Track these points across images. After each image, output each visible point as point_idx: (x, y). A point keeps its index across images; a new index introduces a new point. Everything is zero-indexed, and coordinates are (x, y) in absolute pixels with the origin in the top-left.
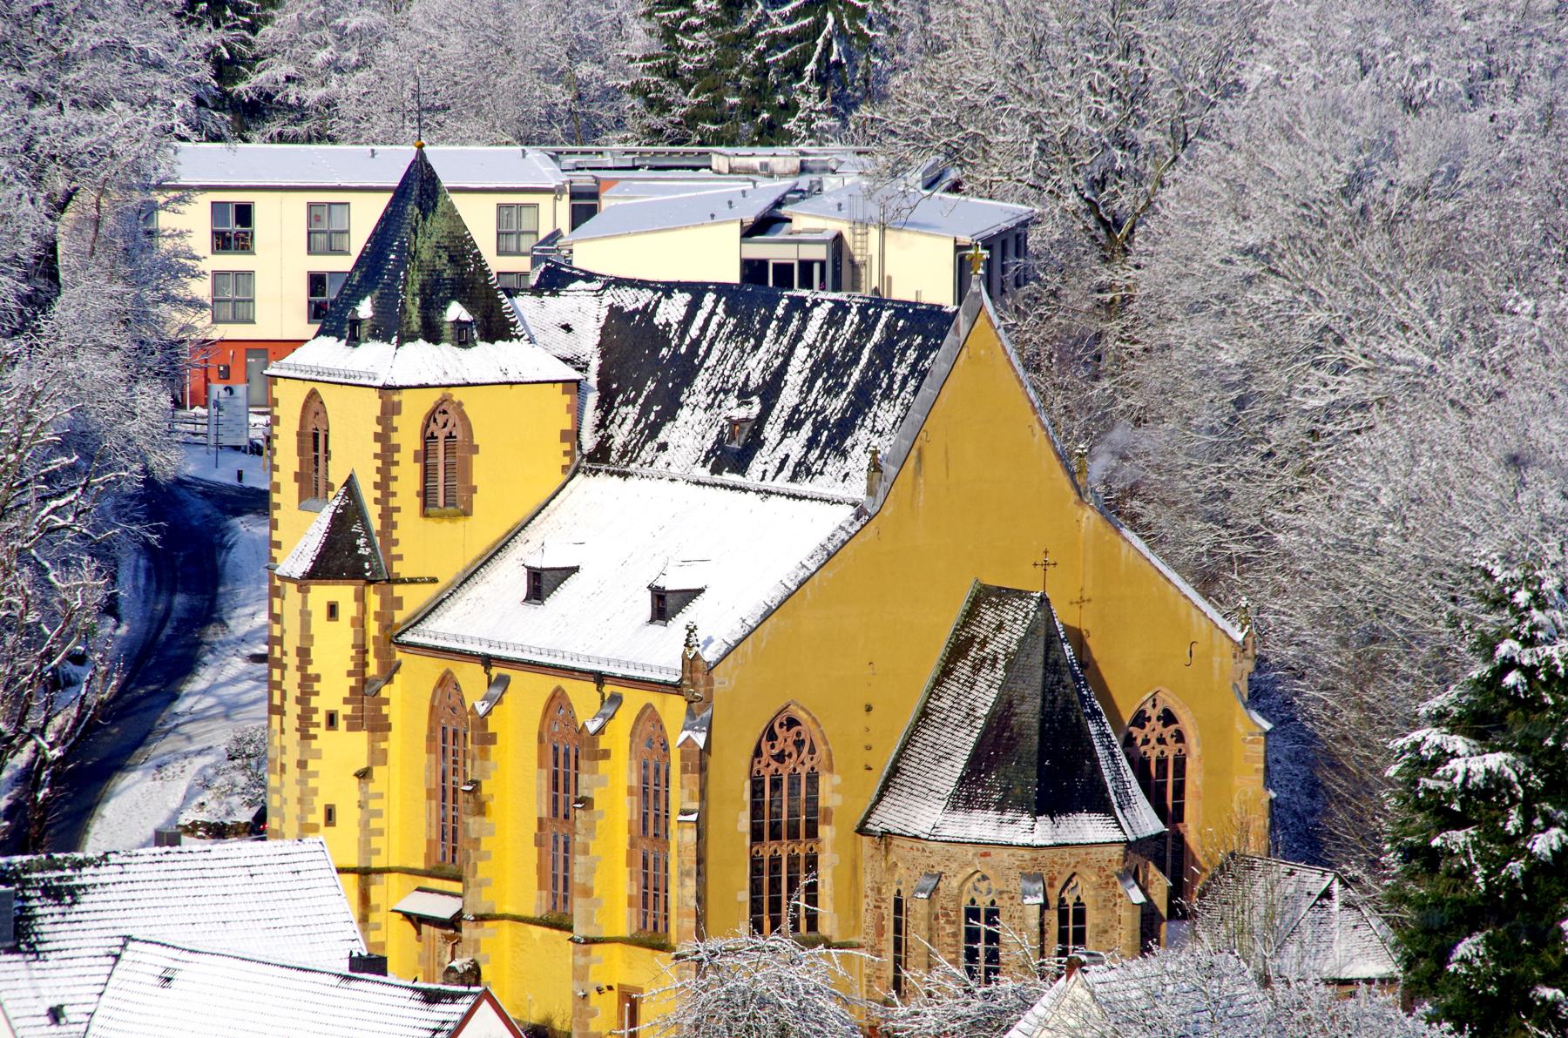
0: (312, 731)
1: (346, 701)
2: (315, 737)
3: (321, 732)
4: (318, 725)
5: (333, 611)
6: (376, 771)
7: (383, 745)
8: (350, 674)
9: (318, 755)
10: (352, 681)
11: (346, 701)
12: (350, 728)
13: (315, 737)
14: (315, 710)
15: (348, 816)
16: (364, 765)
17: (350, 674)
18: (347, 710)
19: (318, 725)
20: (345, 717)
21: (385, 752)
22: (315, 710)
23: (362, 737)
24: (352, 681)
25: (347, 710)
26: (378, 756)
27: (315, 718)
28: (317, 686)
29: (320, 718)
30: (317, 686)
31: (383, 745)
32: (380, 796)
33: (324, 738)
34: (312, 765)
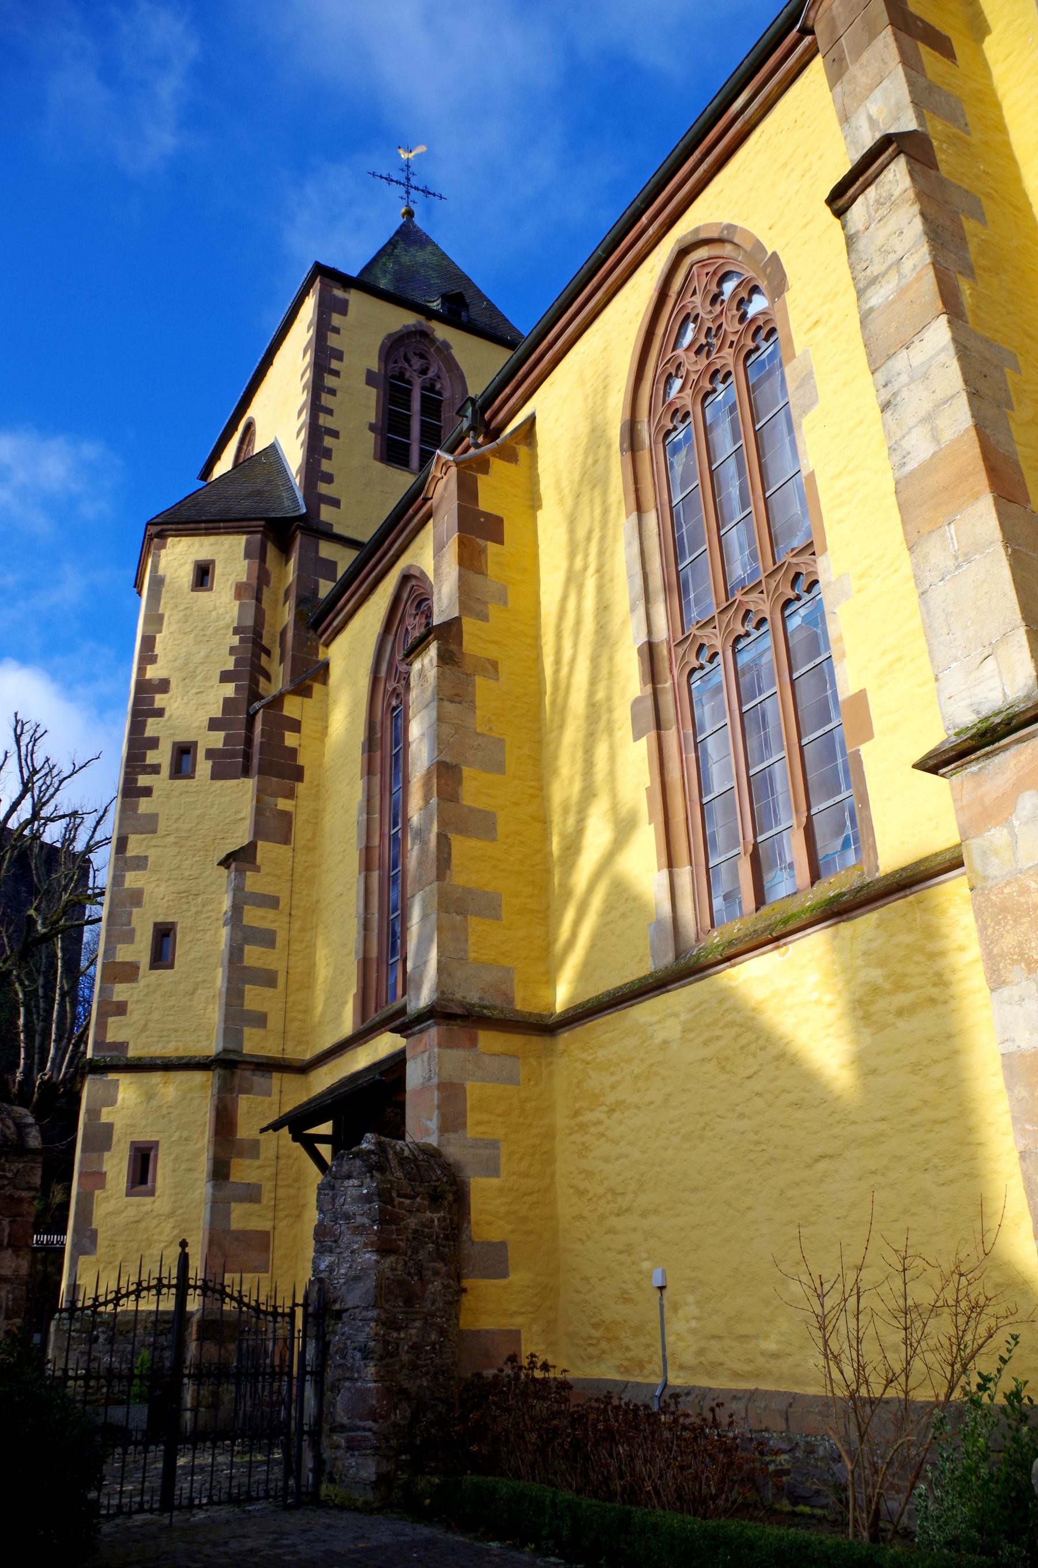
2: (147, 792)
3: (160, 782)
4: (155, 769)
5: (203, 575)
7: (283, 804)
8: (226, 677)
10: (229, 690)
11: (214, 725)
13: (147, 792)
14: (154, 743)
15: (203, 945)
16: (241, 837)
17: (226, 677)
18: (217, 739)
19: (155, 769)
20: (210, 754)
21: (287, 818)
22: (154, 743)
24: (229, 690)
25: (217, 739)
26: (274, 825)
27: (152, 757)
28: (160, 700)
29: (161, 756)
30: (160, 700)
31: (283, 804)
32: (272, 902)
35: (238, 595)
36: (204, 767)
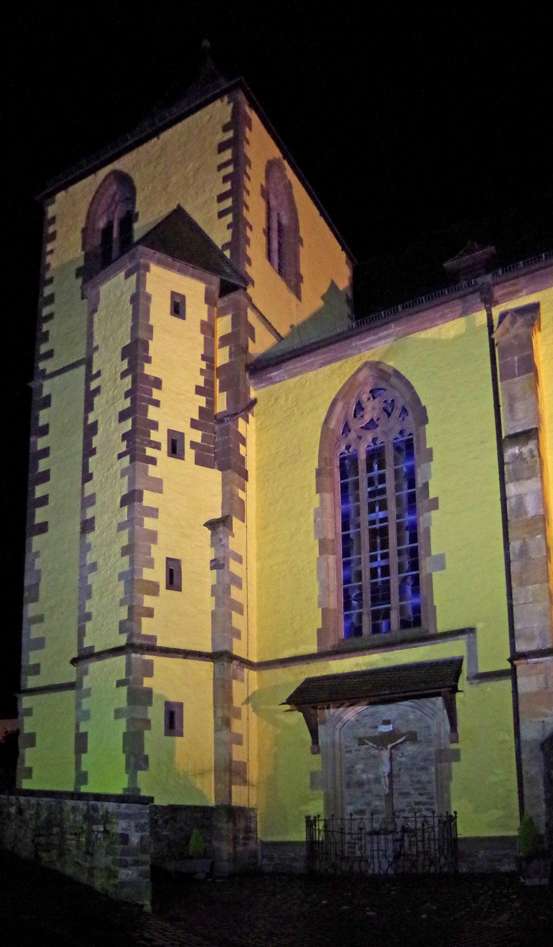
0: (150, 452)
1: (194, 424)
2: (153, 461)
6: (236, 522)
8: (199, 391)
9: (157, 486)
10: (202, 401)
12: (200, 461)
13: (153, 461)
17: (199, 391)
18: (196, 436)
20: (193, 445)
23: (213, 477)
24: (202, 401)
33: (164, 466)
34: (149, 499)
35: (203, 331)
36: (190, 453)
